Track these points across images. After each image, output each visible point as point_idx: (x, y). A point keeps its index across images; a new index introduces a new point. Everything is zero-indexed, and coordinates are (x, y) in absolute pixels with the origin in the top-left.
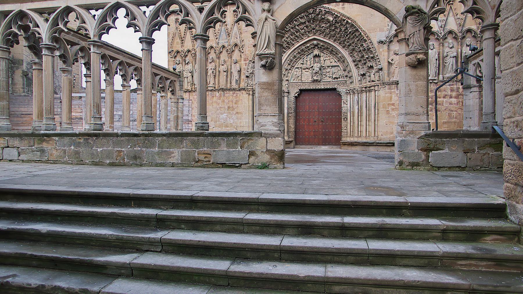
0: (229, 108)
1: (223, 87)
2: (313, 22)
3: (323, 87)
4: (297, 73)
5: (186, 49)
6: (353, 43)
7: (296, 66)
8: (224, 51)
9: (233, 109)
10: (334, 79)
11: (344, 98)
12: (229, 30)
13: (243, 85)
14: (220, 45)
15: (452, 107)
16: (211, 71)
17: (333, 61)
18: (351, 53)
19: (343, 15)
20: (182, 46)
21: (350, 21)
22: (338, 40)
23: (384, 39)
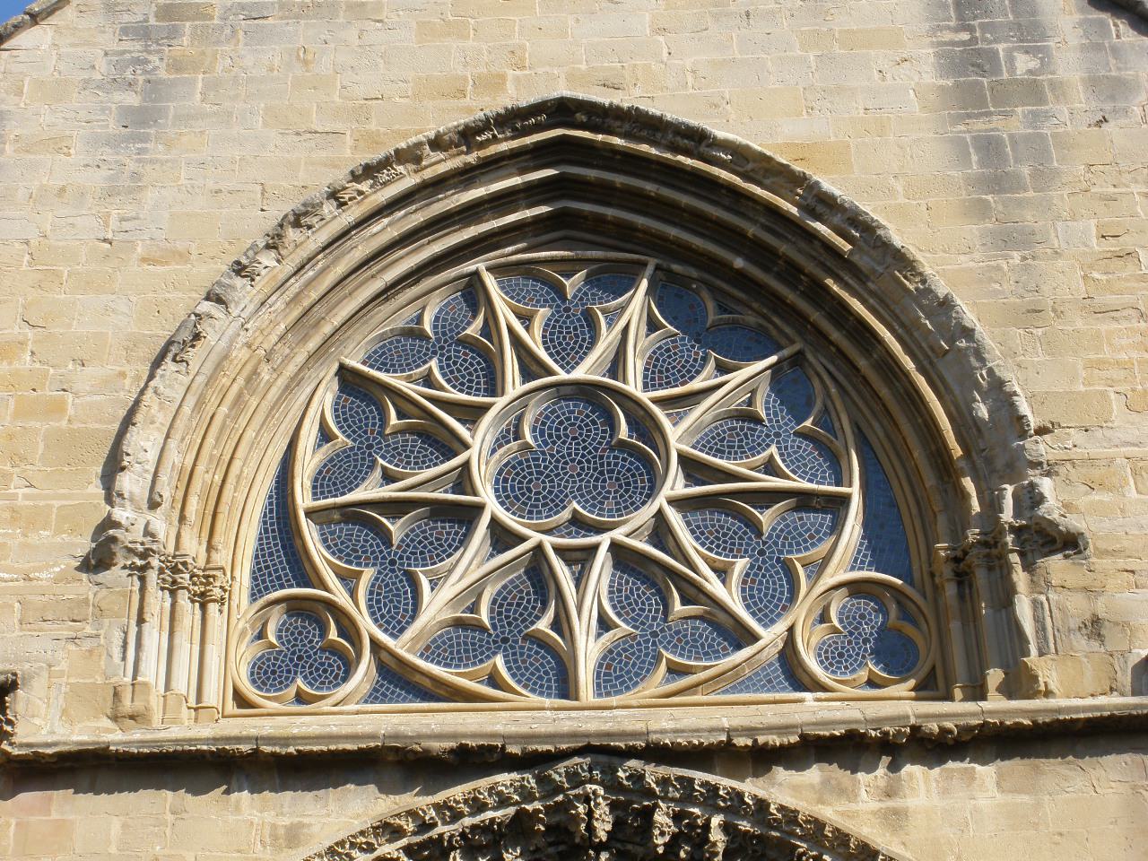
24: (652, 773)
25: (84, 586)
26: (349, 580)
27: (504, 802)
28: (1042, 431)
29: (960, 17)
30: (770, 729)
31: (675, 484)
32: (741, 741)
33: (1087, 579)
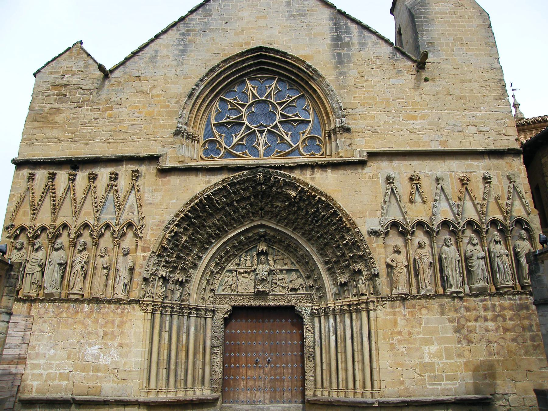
0: (105, 334)
1: (98, 295)
2: (262, 198)
3: (272, 304)
4: (230, 279)
5: (38, 225)
6: (326, 233)
7: (227, 268)
8: (108, 234)
9: (114, 337)
10: (291, 291)
11: (307, 321)
12: (121, 199)
13: (135, 294)
14: (102, 222)
15: (492, 336)
16: (80, 265)
17: (289, 262)
18: (322, 249)
19: (314, 189)
20: (34, 219)
21: (323, 199)
22: (302, 229)
23: (377, 228)
24: (271, 170)
25: (173, 139)
26: (220, 136)
27: (245, 176)
28: (344, 109)
29: (336, 30)
30: (291, 163)
31: (278, 118)
32: (286, 165)
33: (350, 136)
